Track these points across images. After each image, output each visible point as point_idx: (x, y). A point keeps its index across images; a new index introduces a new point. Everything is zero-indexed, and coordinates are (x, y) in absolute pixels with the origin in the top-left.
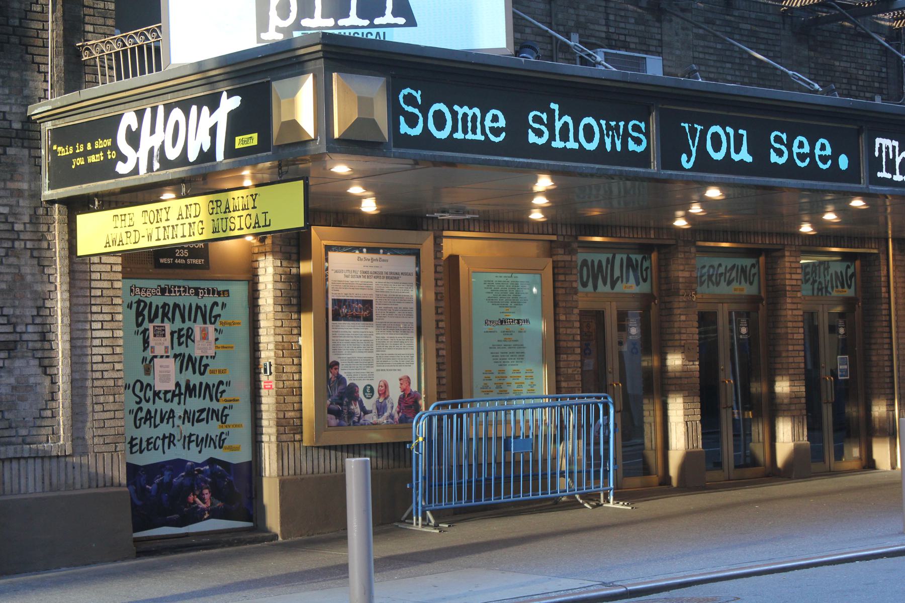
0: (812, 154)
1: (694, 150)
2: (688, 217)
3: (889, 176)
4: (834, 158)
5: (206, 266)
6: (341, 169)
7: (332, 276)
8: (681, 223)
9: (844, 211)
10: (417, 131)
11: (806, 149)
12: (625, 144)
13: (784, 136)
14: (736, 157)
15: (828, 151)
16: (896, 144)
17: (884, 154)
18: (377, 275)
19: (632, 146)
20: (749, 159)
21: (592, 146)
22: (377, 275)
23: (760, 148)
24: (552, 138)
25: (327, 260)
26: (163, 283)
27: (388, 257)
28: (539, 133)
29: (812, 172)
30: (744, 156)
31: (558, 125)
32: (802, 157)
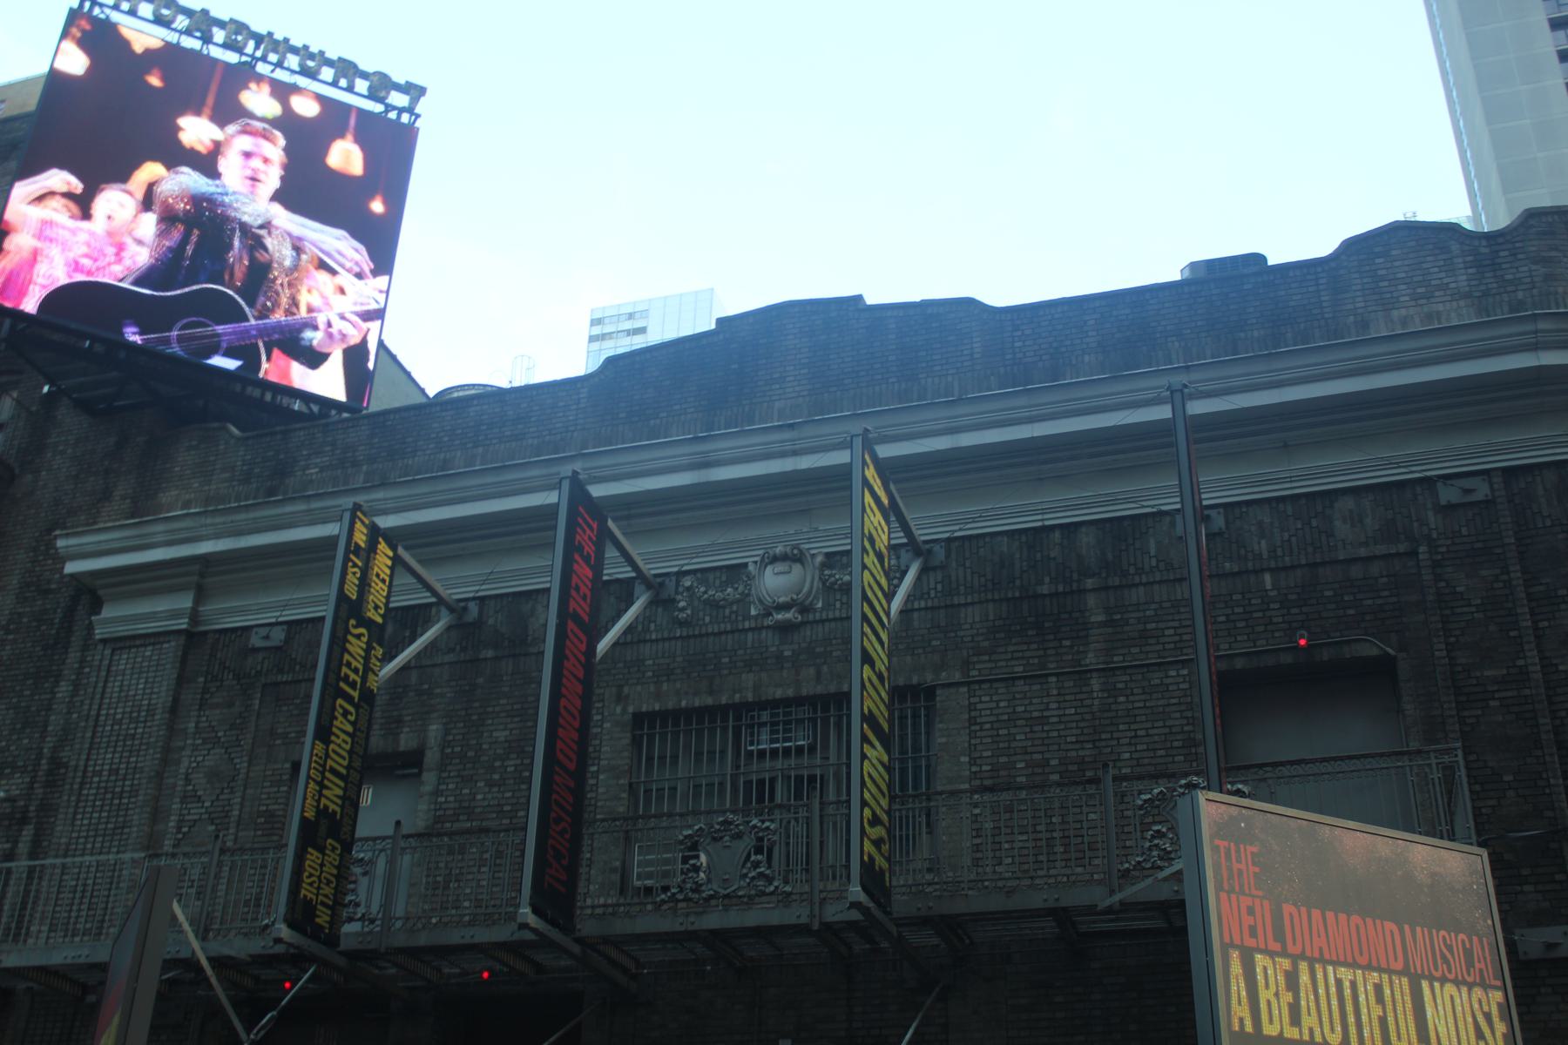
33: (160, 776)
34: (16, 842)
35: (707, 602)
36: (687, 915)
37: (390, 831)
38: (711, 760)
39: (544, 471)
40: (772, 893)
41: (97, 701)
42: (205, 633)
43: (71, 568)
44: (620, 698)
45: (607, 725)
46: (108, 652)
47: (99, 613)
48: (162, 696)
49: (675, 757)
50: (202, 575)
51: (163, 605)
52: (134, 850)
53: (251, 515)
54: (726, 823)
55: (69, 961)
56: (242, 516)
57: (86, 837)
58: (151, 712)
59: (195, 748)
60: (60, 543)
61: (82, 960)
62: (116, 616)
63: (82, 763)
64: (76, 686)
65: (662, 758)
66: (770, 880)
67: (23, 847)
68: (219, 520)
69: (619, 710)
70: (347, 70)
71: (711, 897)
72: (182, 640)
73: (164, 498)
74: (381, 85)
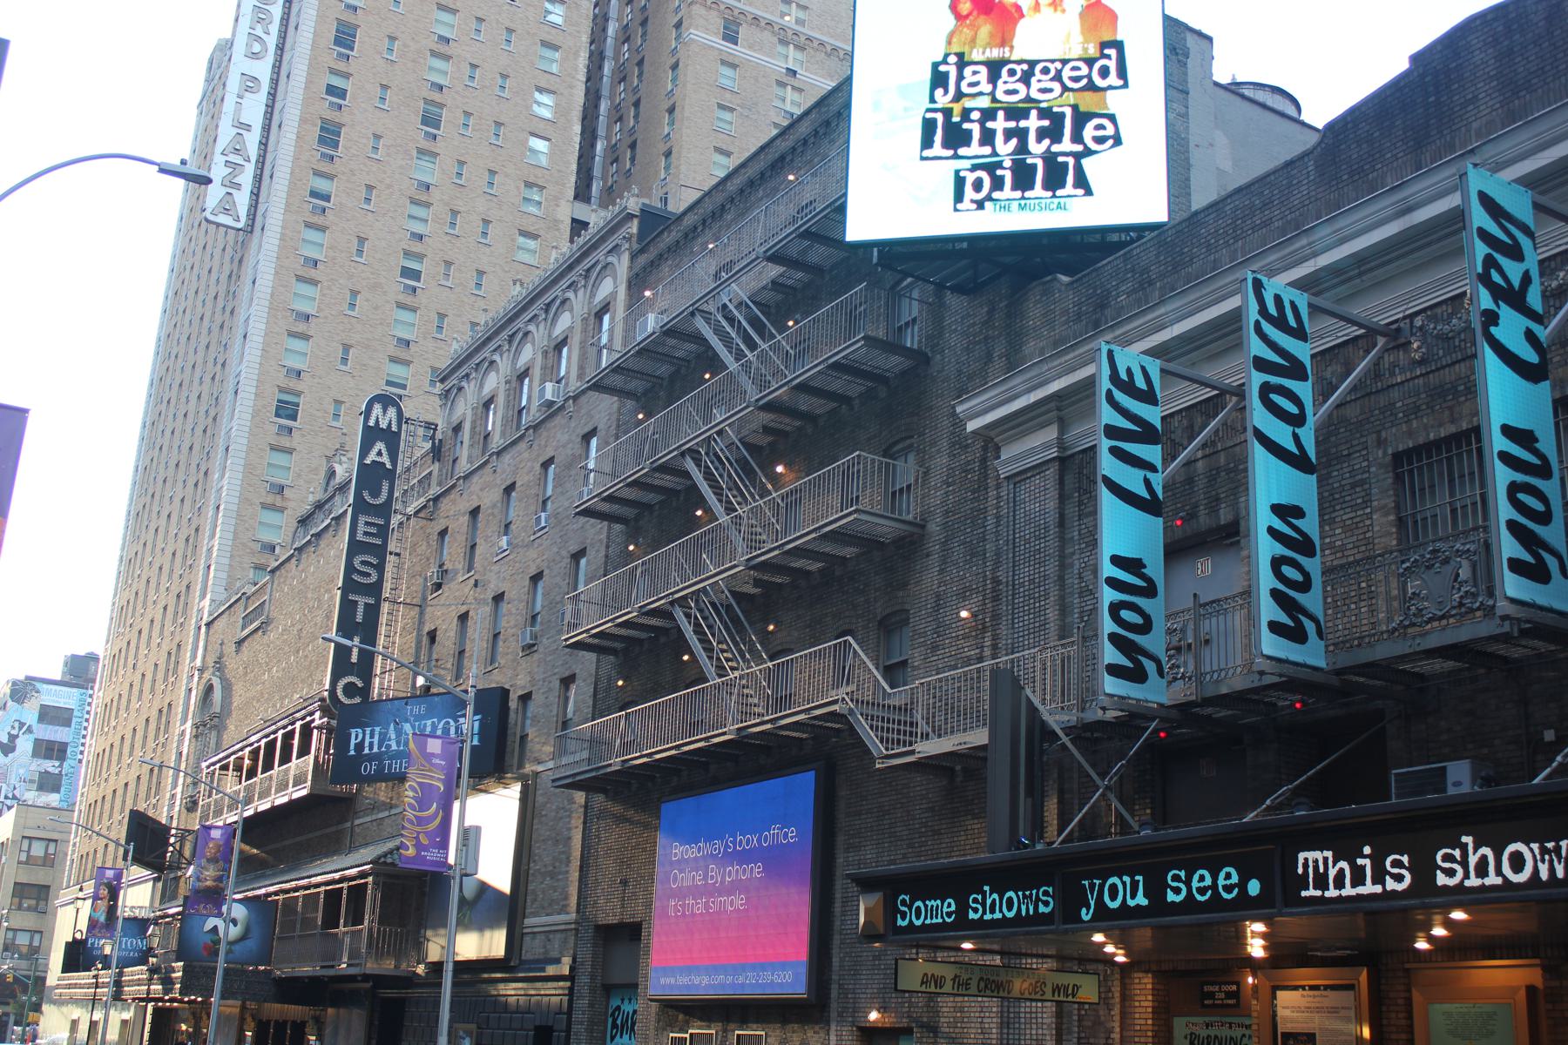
0: (1214, 886)
1: (1092, 903)
2: (1431, 939)
3: (1318, 893)
4: (1242, 885)
5: (1237, 1005)
6: (1098, 938)
7: (1281, 1012)
8: (1422, 945)
9: (1448, 924)
10: (905, 923)
11: (1208, 881)
12: (1036, 908)
13: (1182, 874)
14: (1131, 903)
15: (1235, 879)
16: (1329, 854)
17: (1311, 870)
18: (1319, 1010)
19: (1042, 909)
20: (1144, 902)
21: (1010, 915)
22: (1319, 1010)
23: (1156, 890)
24: (984, 912)
25: (1275, 997)
26: (1207, 1019)
27: (1328, 993)
28: (976, 910)
29: (1216, 902)
30: (1141, 900)
31: (989, 902)
32: (1202, 891)
33: (1061, 579)
35: (1438, 337)
36: (1414, 638)
37: (1191, 605)
38: (1462, 484)
40: (1479, 609)
42: (1073, 455)
43: (971, 426)
44: (1380, 443)
45: (1373, 469)
49: (1432, 486)
50: (1059, 409)
54: (1434, 551)
56: (1071, 355)
60: (959, 409)
65: (1422, 490)
66: (1475, 596)
67: (987, 652)
69: (1380, 453)
71: (1430, 620)
73: (1027, 350)
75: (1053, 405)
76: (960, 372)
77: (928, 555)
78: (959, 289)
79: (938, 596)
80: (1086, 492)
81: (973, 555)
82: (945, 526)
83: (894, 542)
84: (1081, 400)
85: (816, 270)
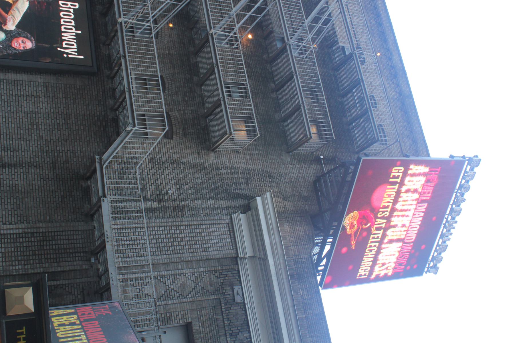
34: (151, 200)
39: (290, 304)
41: (208, 222)
42: (237, 264)
43: (259, 200)
46: (227, 221)
47: (242, 213)
48: (214, 253)
50: (259, 258)
51: (247, 243)
52: (152, 259)
53: (285, 280)
55: (110, 276)
56: (284, 277)
57: (155, 235)
58: (205, 250)
59: (193, 273)
60: (268, 194)
61: (111, 282)
62: (241, 220)
63: (184, 223)
64: (214, 208)
67: (149, 204)
68: (282, 267)
70: (444, 248)
72: (234, 255)
74: (438, 259)
75: (263, 256)
76: (281, 176)
77: (199, 153)
78: (318, 180)
79: (178, 163)
80: (221, 274)
81: (196, 189)
82: (212, 167)
83: (207, 125)
84: (262, 272)
85: (337, 68)
